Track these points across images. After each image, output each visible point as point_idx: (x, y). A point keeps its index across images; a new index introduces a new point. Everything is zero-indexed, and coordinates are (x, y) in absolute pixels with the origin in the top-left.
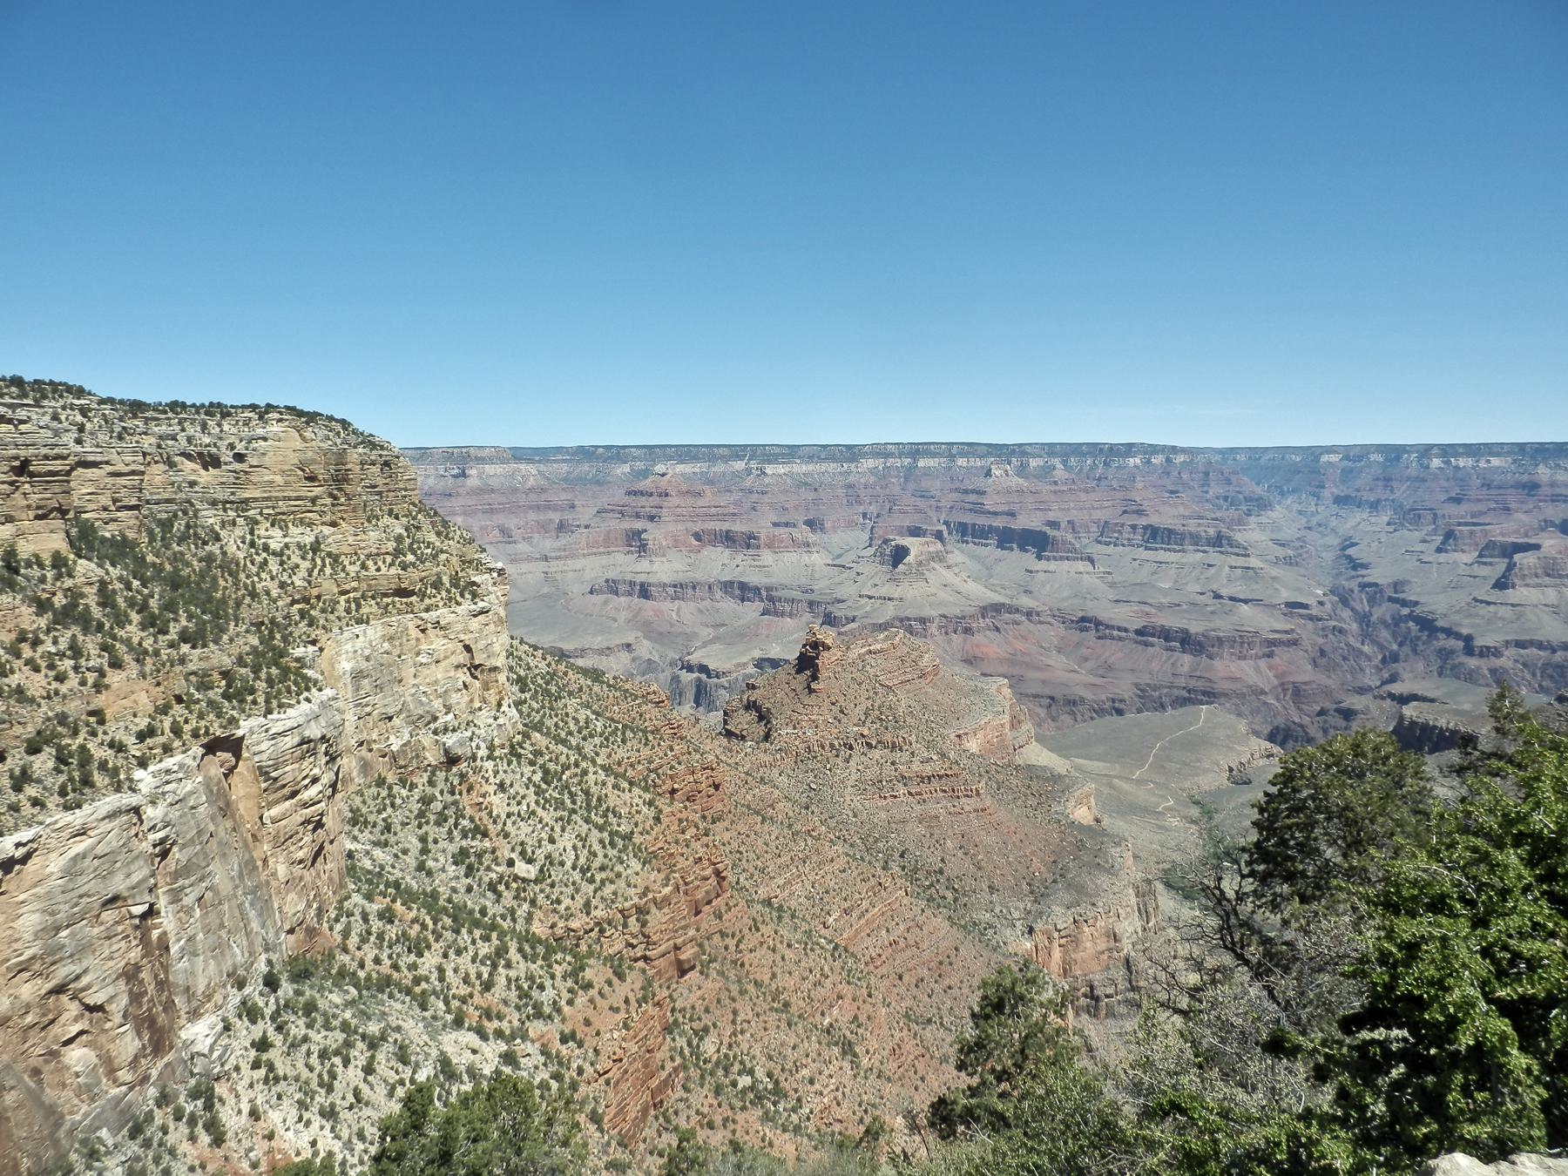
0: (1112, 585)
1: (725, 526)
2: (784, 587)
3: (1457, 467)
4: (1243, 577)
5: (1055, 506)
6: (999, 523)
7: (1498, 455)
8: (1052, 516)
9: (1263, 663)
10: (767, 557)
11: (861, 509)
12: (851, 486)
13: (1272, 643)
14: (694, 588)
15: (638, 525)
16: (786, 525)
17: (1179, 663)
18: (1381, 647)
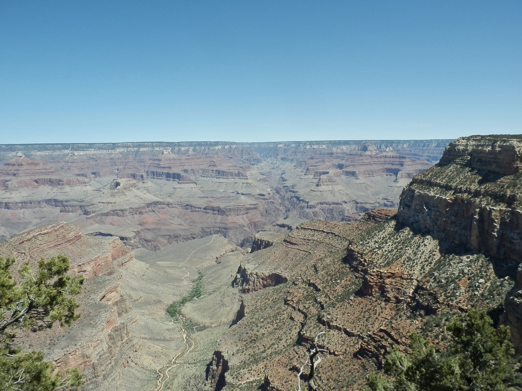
0: (203, 191)
1: (49, 177)
2: (74, 200)
3: (314, 148)
4: (246, 186)
5: (187, 164)
6: (165, 171)
7: (324, 144)
8: (185, 168)
9: (245, 216)
10: (67, 188)
11: (116, 167)
12: (112, 159)
13: (248, 209)
14: (31, 203)
15: (8, 178)
16: (83, 175)
17: (214, 219)
18: (286, 207)
